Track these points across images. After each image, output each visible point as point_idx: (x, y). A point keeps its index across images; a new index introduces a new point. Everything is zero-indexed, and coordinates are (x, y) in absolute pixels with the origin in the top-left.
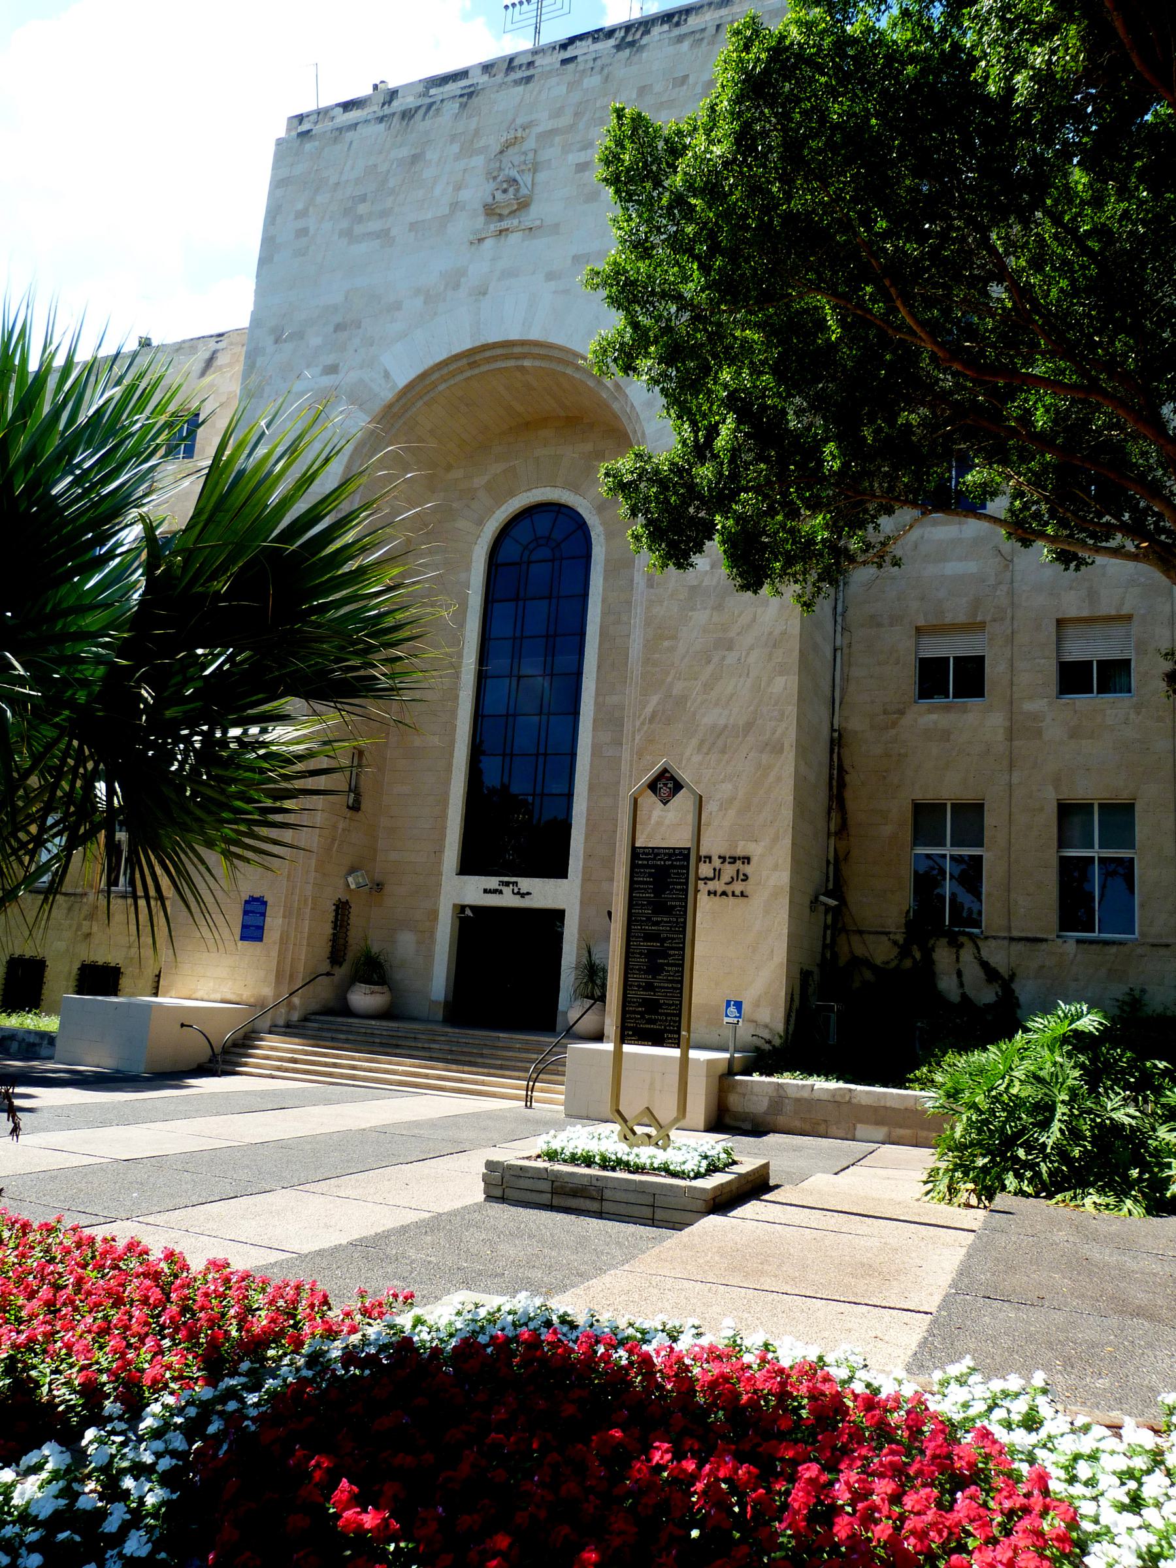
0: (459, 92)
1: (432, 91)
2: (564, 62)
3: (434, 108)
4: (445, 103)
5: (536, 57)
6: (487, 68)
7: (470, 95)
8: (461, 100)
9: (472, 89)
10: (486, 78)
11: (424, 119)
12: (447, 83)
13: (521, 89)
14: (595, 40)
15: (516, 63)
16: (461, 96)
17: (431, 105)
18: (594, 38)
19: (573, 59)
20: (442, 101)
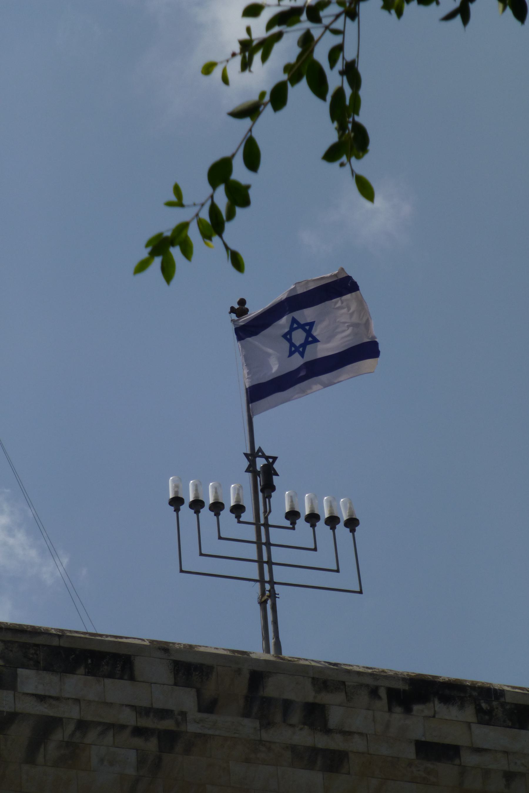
0: (128, 718)
1: (31, 680)
2: (427, 750)
3: (58, 736)
4: (92, 736)
5: (325, 698)
6: (189, 668)
7: (169, 739)
8: (138, 742)
9: (168, 724)
10: (185, 700)
11: (30, 758)
12: (70, 670)
13: (316, 778)
14: (486, 717)
15: (271, 689)
16: (139, 732)
17: (47, 726)
18: (479, 710)
19: (448, 752)
20: (82, 725)
